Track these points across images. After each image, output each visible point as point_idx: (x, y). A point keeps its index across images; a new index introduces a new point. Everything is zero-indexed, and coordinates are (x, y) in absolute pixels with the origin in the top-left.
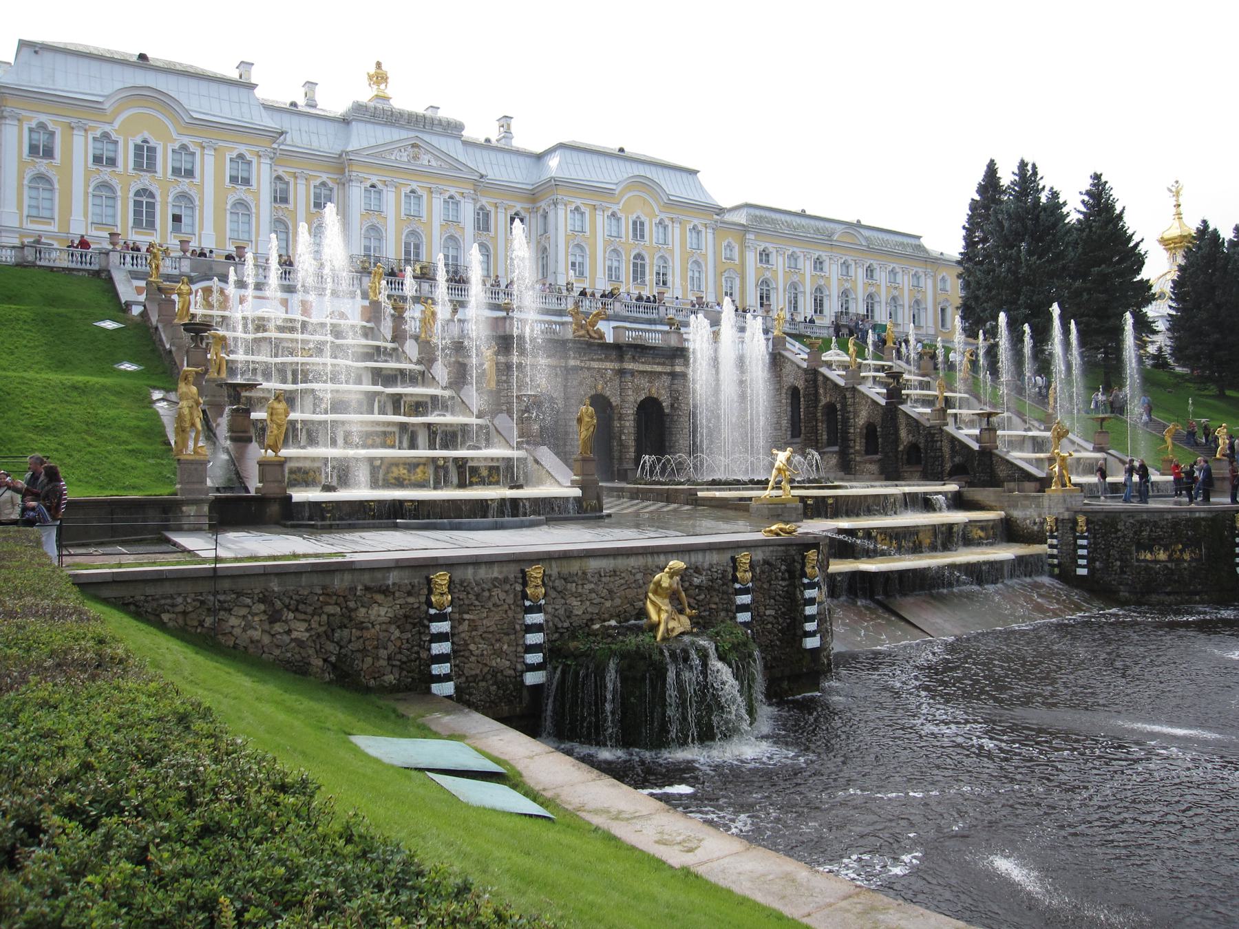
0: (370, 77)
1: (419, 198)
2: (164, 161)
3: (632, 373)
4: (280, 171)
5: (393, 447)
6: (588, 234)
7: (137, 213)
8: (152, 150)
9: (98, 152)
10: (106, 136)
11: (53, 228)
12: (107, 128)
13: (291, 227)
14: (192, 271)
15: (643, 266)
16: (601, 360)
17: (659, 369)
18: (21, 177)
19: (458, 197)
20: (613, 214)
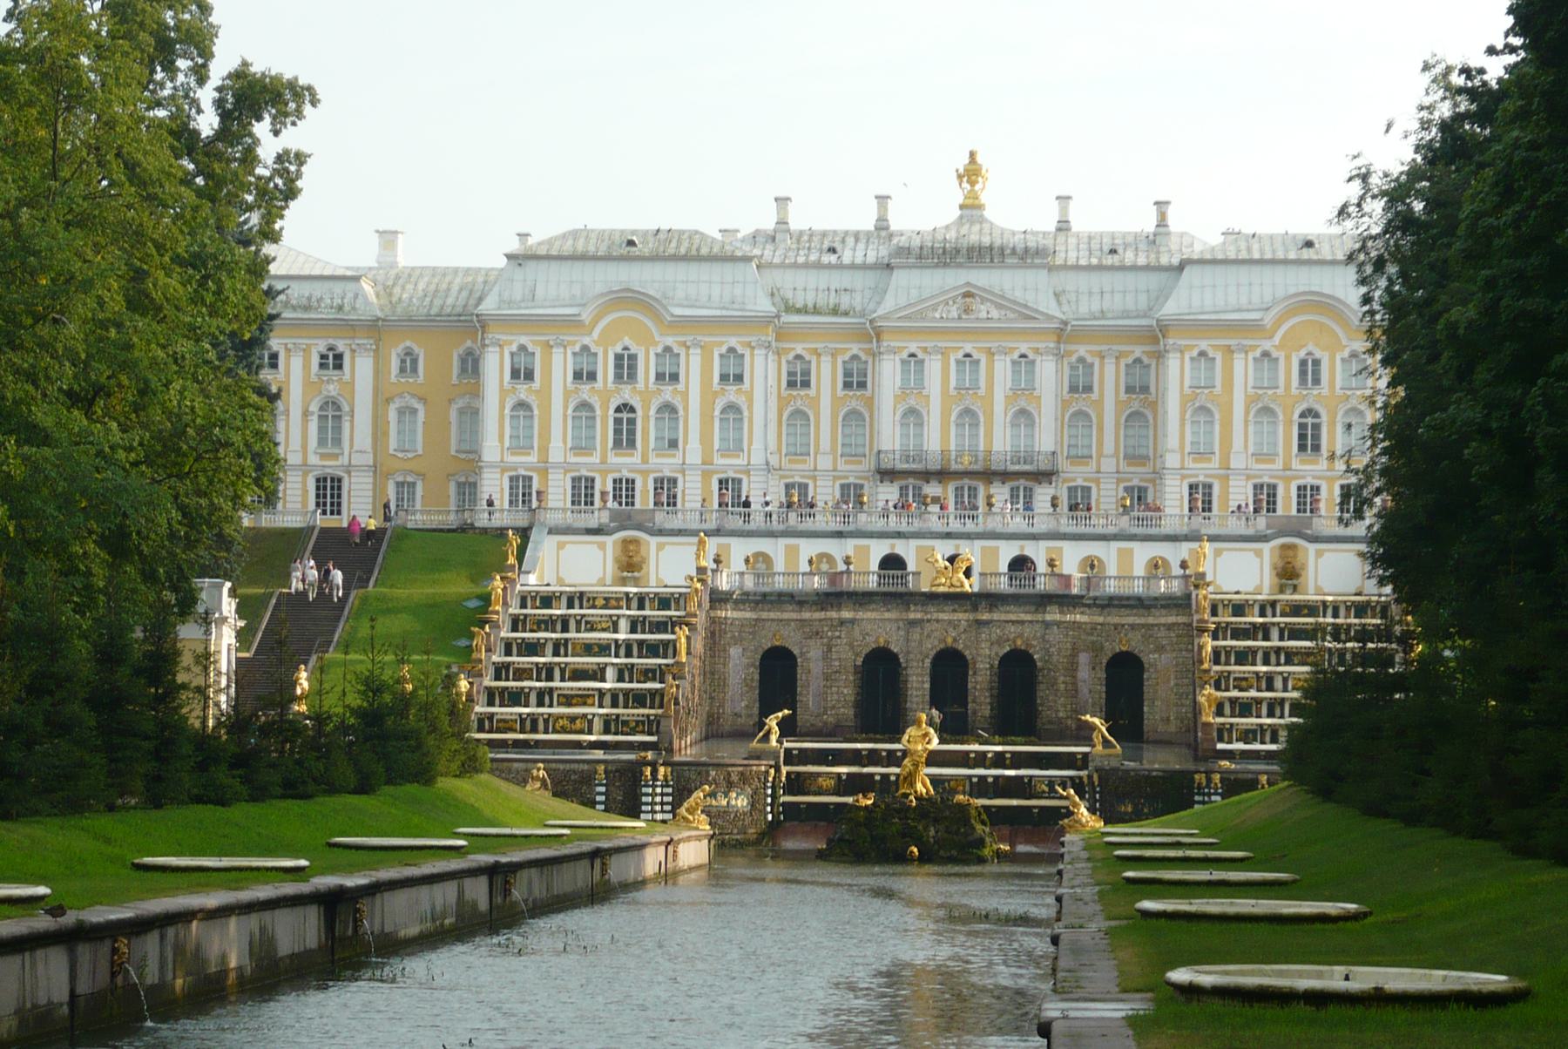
0: (960, 177)
1: (978, 362)
2: (647, 368)
3: (987, 623)
4: (799, 351)
5: (593, 705)
6: (1218, 389)
7: (618, 432)
8: (633, 358)
9: (578, 367)
10: (585, 348)
11: (533, 458)
12: (586, 341)
13: (812, 418)
14: (611, 521)
15: (1316, 427)
16: (954, 611)
17: (1028, 617)
18: (502, 408)
19: (1031, 356)
20: (1266, 354)
